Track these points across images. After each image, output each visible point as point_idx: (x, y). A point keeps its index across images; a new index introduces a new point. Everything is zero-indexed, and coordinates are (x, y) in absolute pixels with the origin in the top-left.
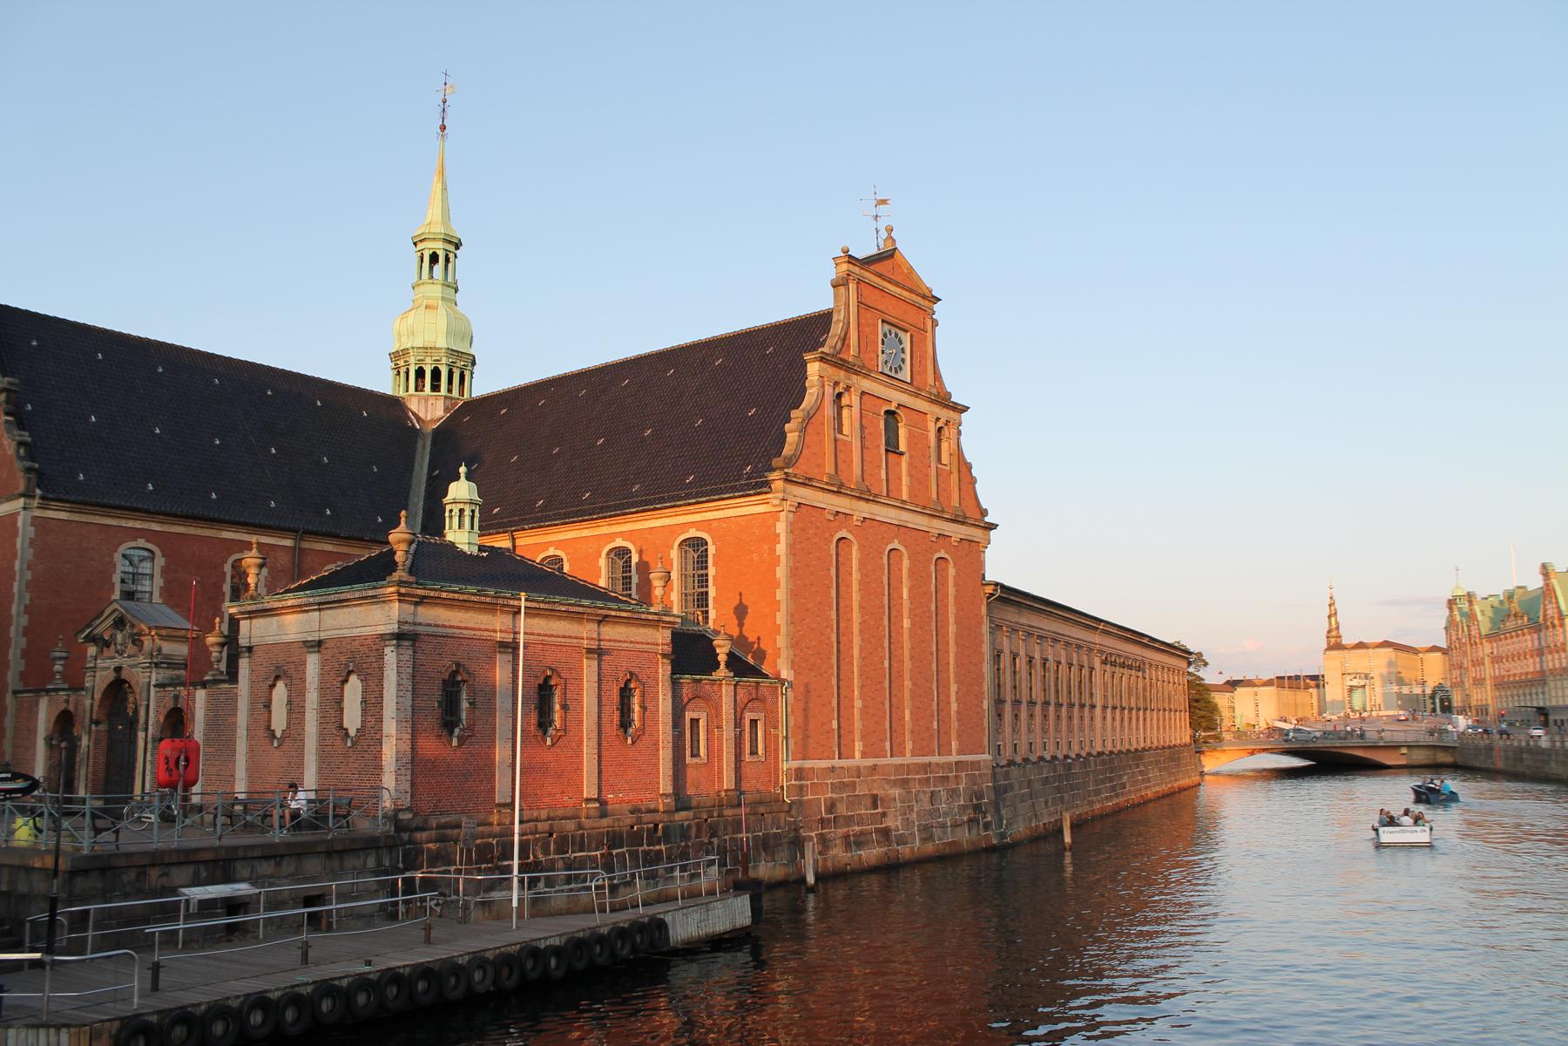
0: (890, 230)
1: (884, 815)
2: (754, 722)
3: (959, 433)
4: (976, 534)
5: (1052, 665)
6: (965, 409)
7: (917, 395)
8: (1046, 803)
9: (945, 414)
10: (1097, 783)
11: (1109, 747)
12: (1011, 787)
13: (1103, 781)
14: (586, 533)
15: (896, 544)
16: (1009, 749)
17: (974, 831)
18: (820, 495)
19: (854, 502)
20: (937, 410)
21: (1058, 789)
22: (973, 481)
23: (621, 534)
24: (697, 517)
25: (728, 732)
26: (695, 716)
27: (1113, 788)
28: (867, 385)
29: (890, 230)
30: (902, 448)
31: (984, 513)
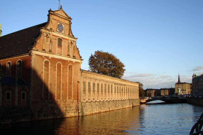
0: (61, 6)
1: (54, 111)
2: (24, 94)
3: (76, 43)
4: (79, 61)
5: (100, 85)
6: (77, 39)
7: (65, 36)
8: (96, 109)
9: (72, 39)
10: (111, 105)
11: (117, 99)
12: (86, 106)
13: (113, 105)
14: (4, 60)
15: (59, 62)
16: (87, 100)
17: (76, 114)
18: (41, 53)
19: (49, 54)
20: (70, 39)
21: (100, 107)
22: (79, 51)
23: (9, 60)
24: (20, 57)
25: (17, 95)
26: (8, 92)
27: (116, 106)
28: (54, 33)
29: (61, 6)
30: (63, 45)
31: (81, 57)
